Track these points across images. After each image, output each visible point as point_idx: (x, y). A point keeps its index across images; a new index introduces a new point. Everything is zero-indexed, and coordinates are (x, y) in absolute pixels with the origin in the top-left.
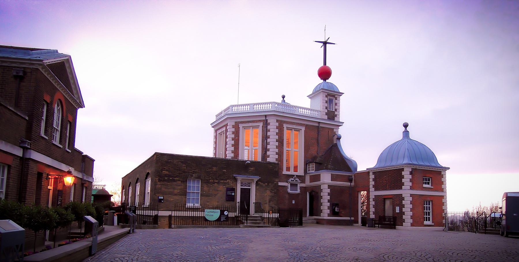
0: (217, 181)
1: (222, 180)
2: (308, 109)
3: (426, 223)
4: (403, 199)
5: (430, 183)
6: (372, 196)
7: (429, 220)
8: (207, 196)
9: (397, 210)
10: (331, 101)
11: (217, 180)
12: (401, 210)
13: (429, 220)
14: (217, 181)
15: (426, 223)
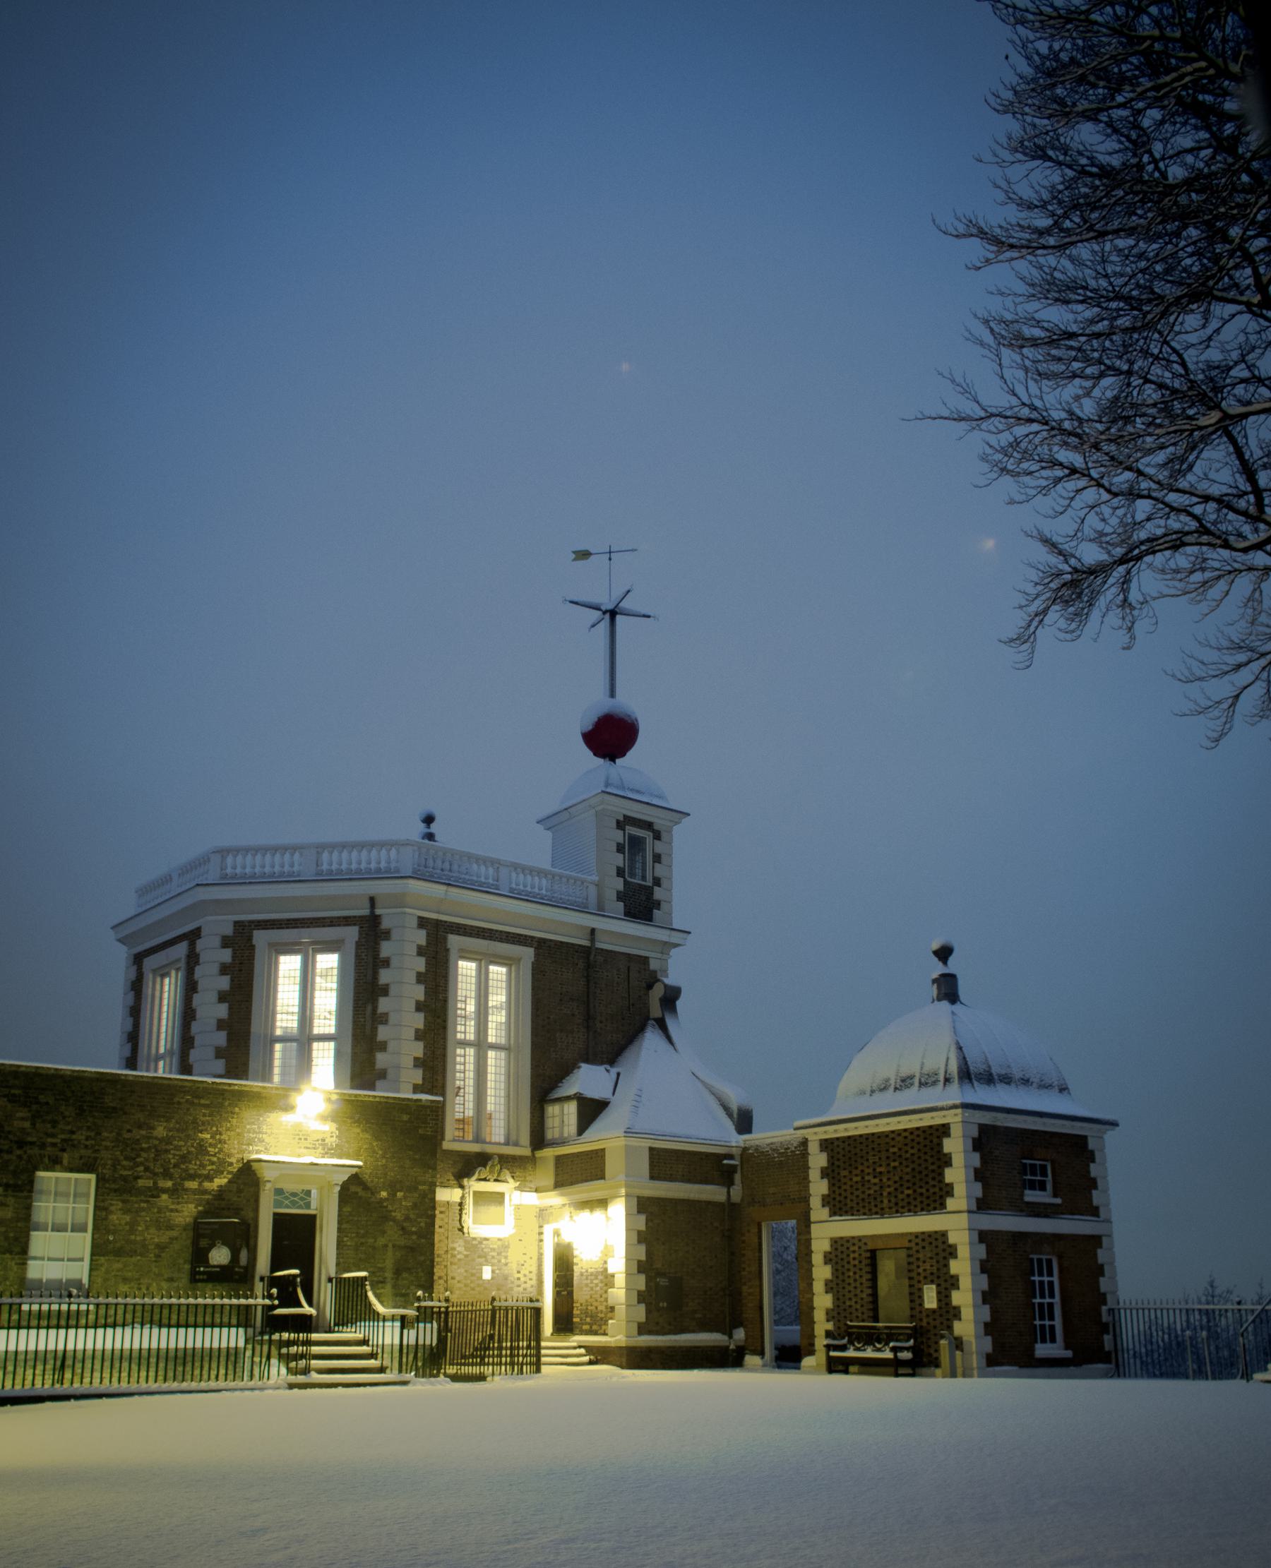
0: (169, 1184)
1: (192, 1177)
2: (541, 873)
3: (1042, 1350)
4: (952, 1252)
5: (1049, 1186)
6: (820, 1246)
7: (1053, 1340)
8: (119, 1253)
9: (930, 1299)
10: (635, 845)
11: (167, 1175)
12: (944, 1297)
13: (1053, 1340)
14: (169, 1184)
15: (1042, 1350)
